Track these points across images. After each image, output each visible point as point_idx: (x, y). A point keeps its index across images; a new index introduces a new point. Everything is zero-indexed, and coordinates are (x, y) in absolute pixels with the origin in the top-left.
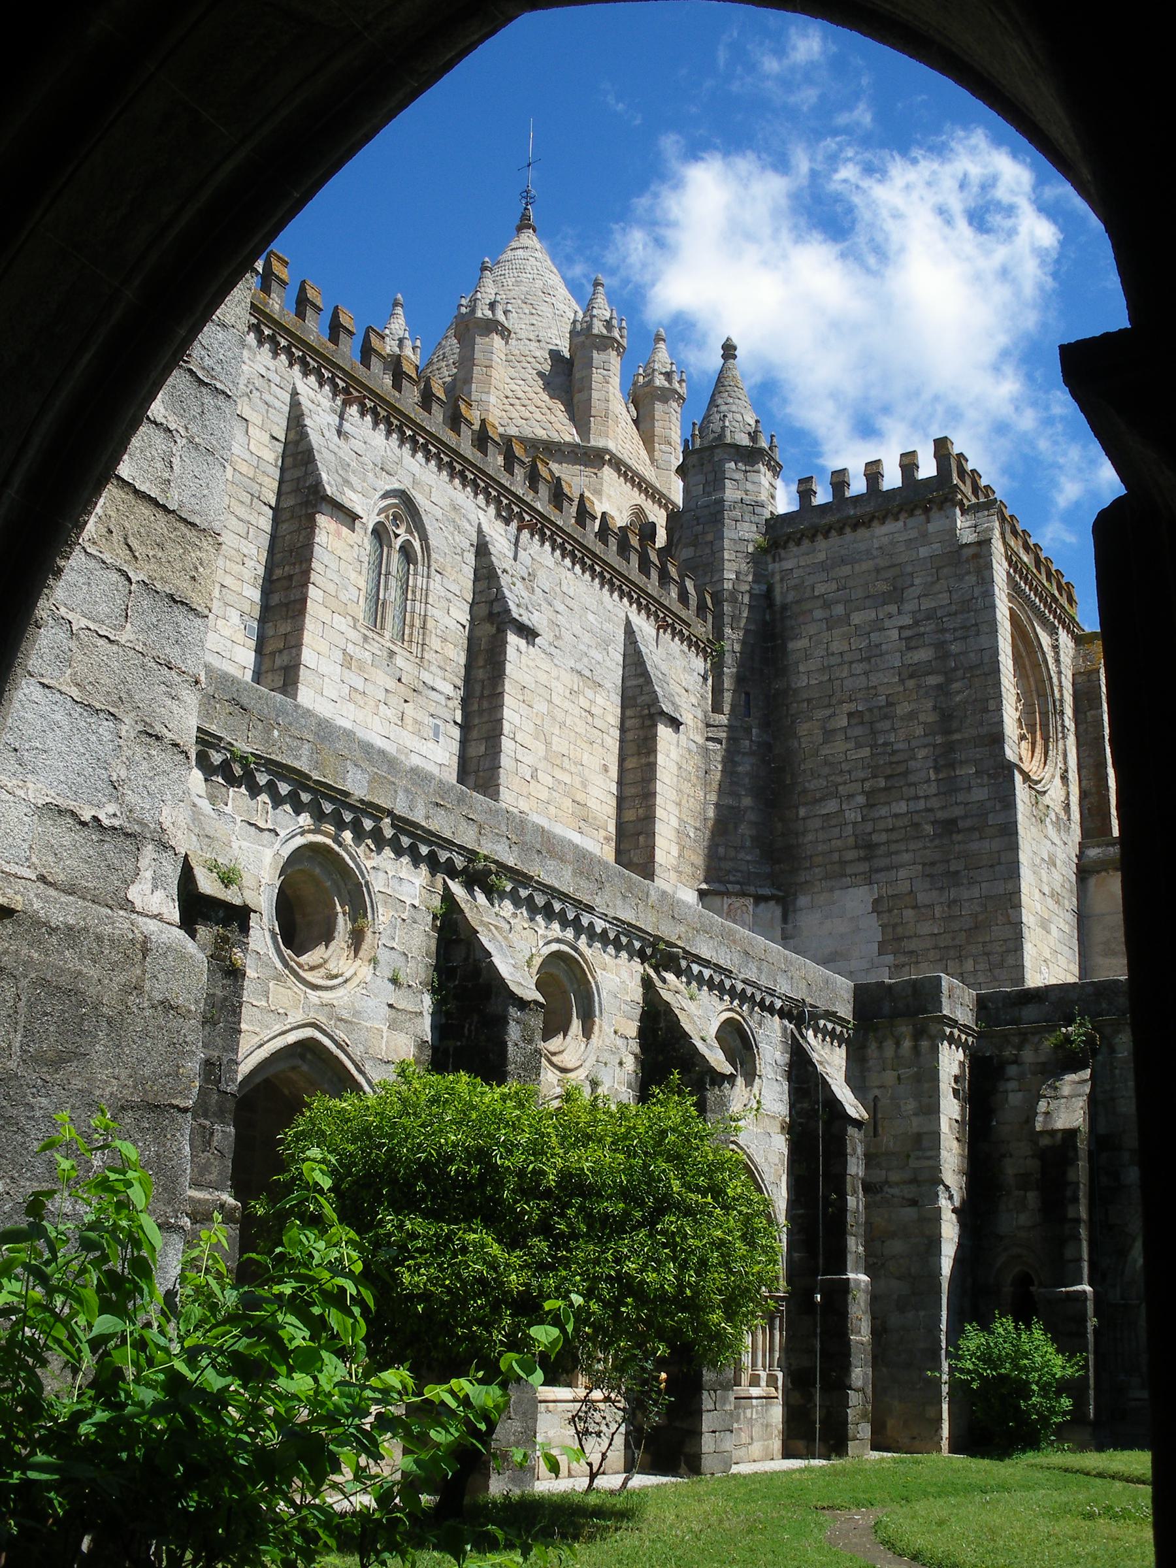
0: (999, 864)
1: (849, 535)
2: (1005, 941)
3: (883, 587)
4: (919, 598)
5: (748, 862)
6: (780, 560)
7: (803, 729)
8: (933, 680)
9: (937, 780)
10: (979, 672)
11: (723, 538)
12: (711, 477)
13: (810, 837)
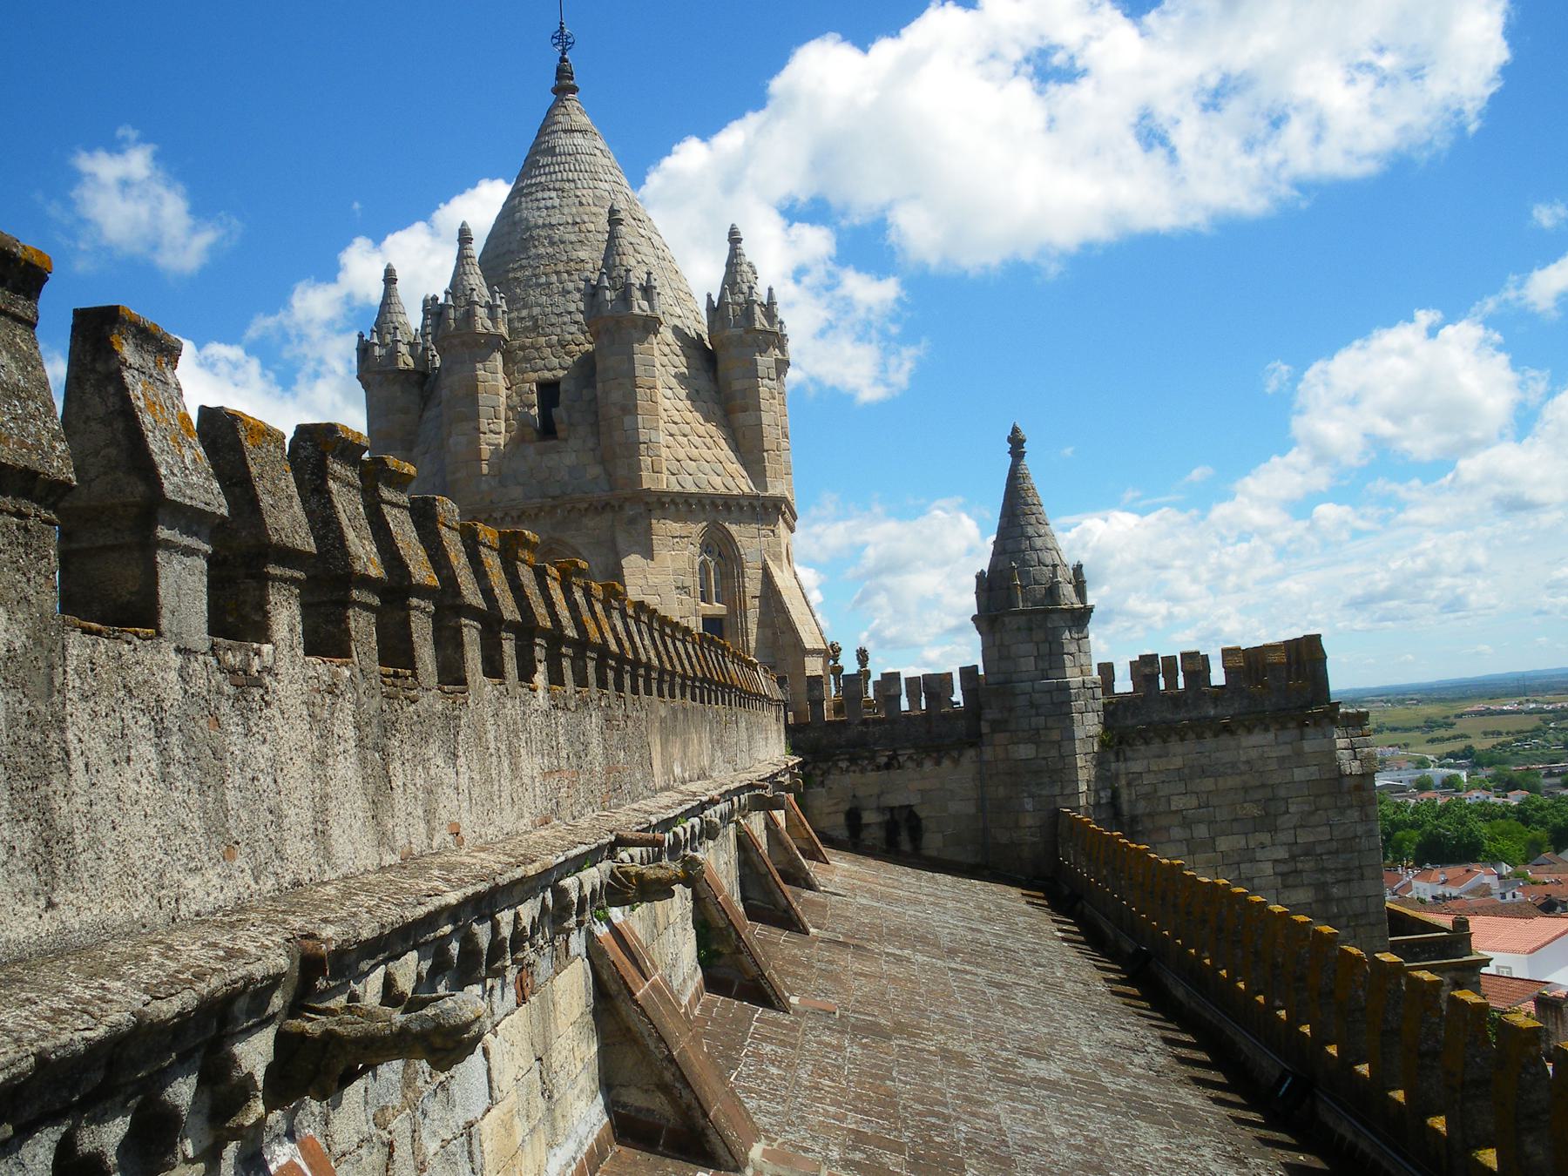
1: (1209, 742)
3: (1256, 812)
4: (1295, 828)
6: (1126, 760)
10: (1363, 922)
11: (1073, 739)
12: (1044, 648)
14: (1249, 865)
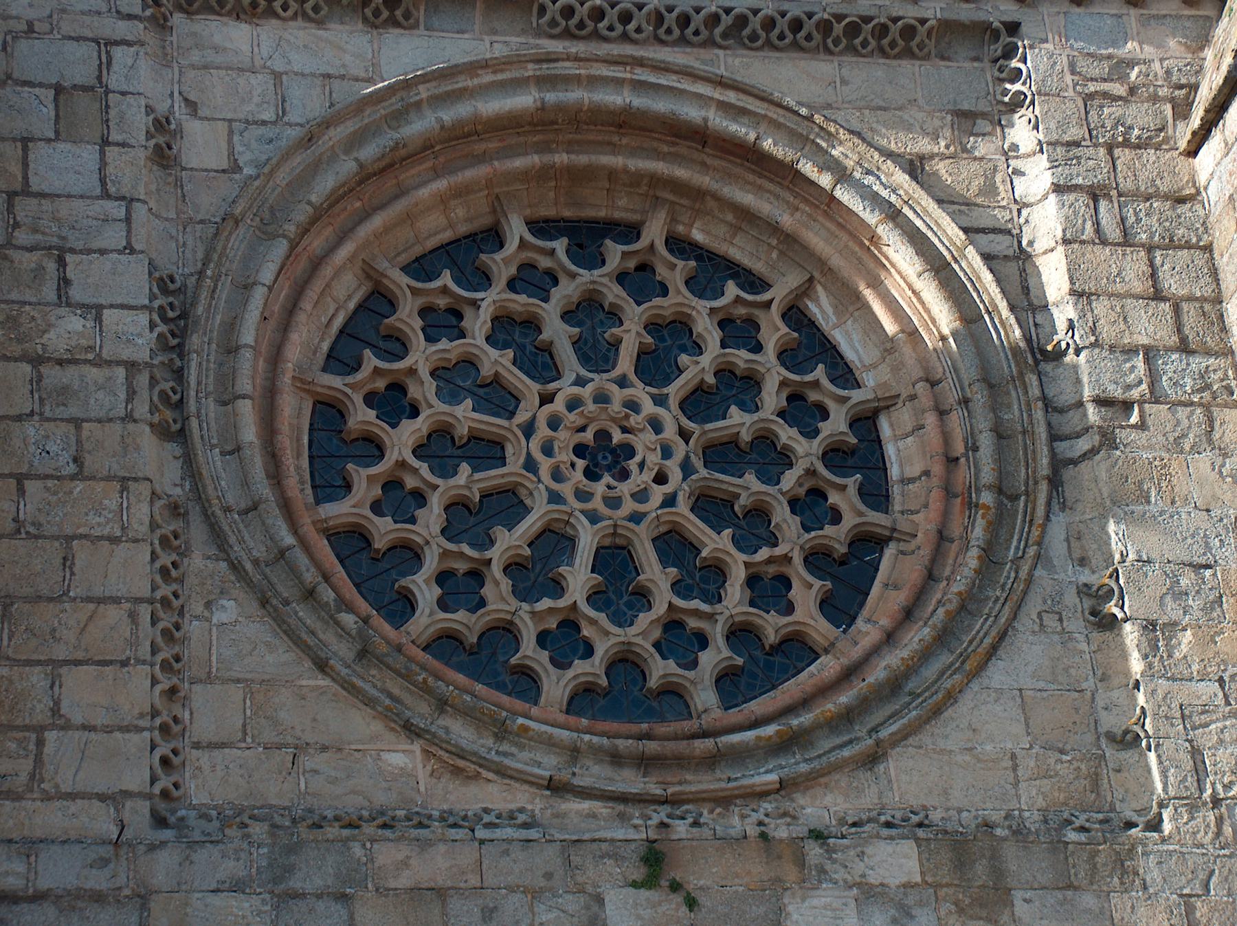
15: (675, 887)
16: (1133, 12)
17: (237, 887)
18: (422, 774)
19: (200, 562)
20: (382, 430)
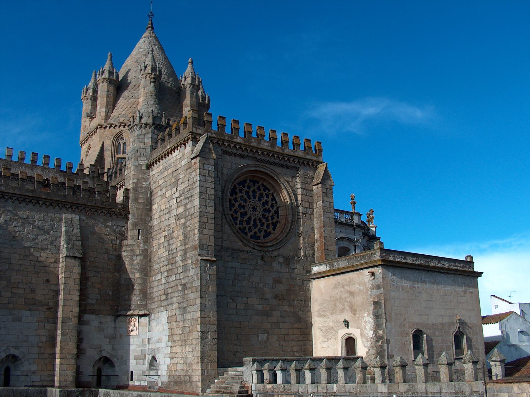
0: (195, 304)
2: (196, 339)
3: (174, 180)
5: (137, 300)
7: (155, 243)
8: (183, 221)
9: (182, 266)
10: (194, 217)
13: (154, 290)
14: (171, 201)
15: (264, 260)
16: (309, 168)
17: (229, 256)
18: (242, 245)
19: (224, 220)
20: (235, 203)
